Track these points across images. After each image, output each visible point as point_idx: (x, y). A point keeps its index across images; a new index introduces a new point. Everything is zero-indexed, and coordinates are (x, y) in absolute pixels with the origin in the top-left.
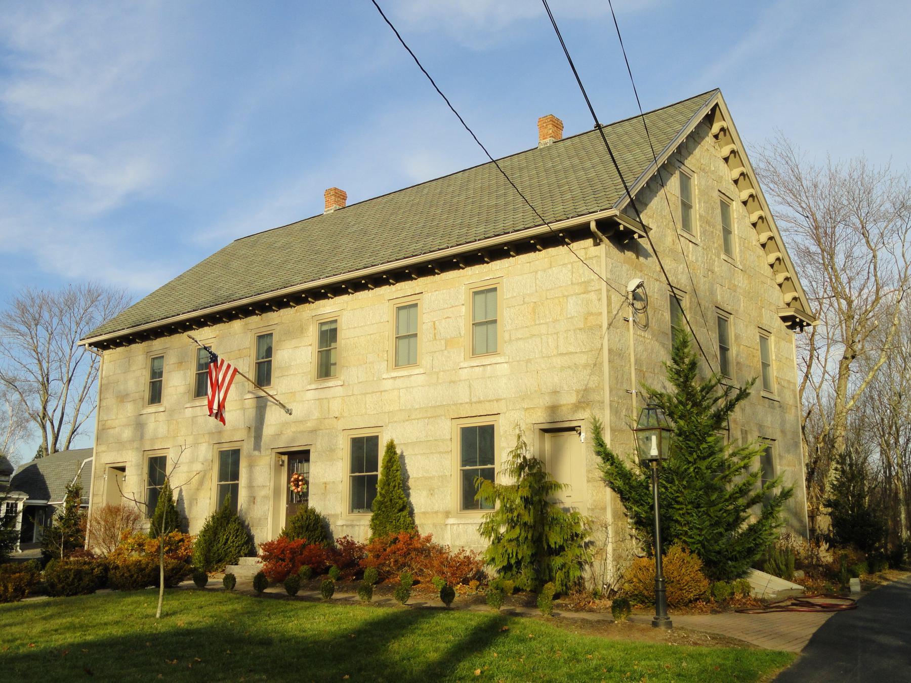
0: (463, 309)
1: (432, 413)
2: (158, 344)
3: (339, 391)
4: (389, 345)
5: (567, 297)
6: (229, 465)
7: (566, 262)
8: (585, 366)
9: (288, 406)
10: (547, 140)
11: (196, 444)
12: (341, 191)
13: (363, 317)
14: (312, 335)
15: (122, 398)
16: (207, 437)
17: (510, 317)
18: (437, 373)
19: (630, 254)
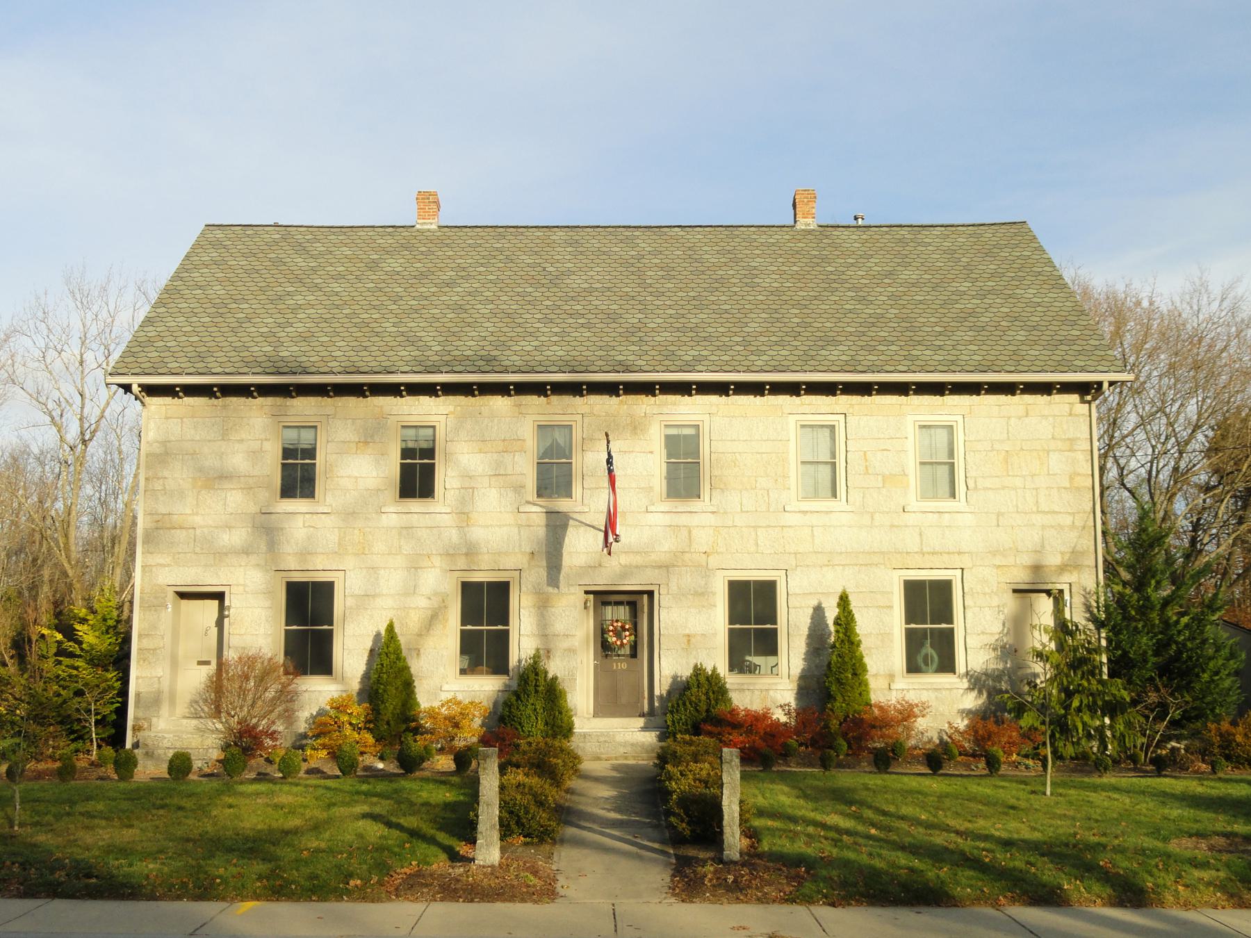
2: (304, 407)
3: (711, 520)
5: (1048, 452)
7: (1046, 413)
11: (414, 567)
14: (655, 439)
15: (217, 479)
16: (437, 561)
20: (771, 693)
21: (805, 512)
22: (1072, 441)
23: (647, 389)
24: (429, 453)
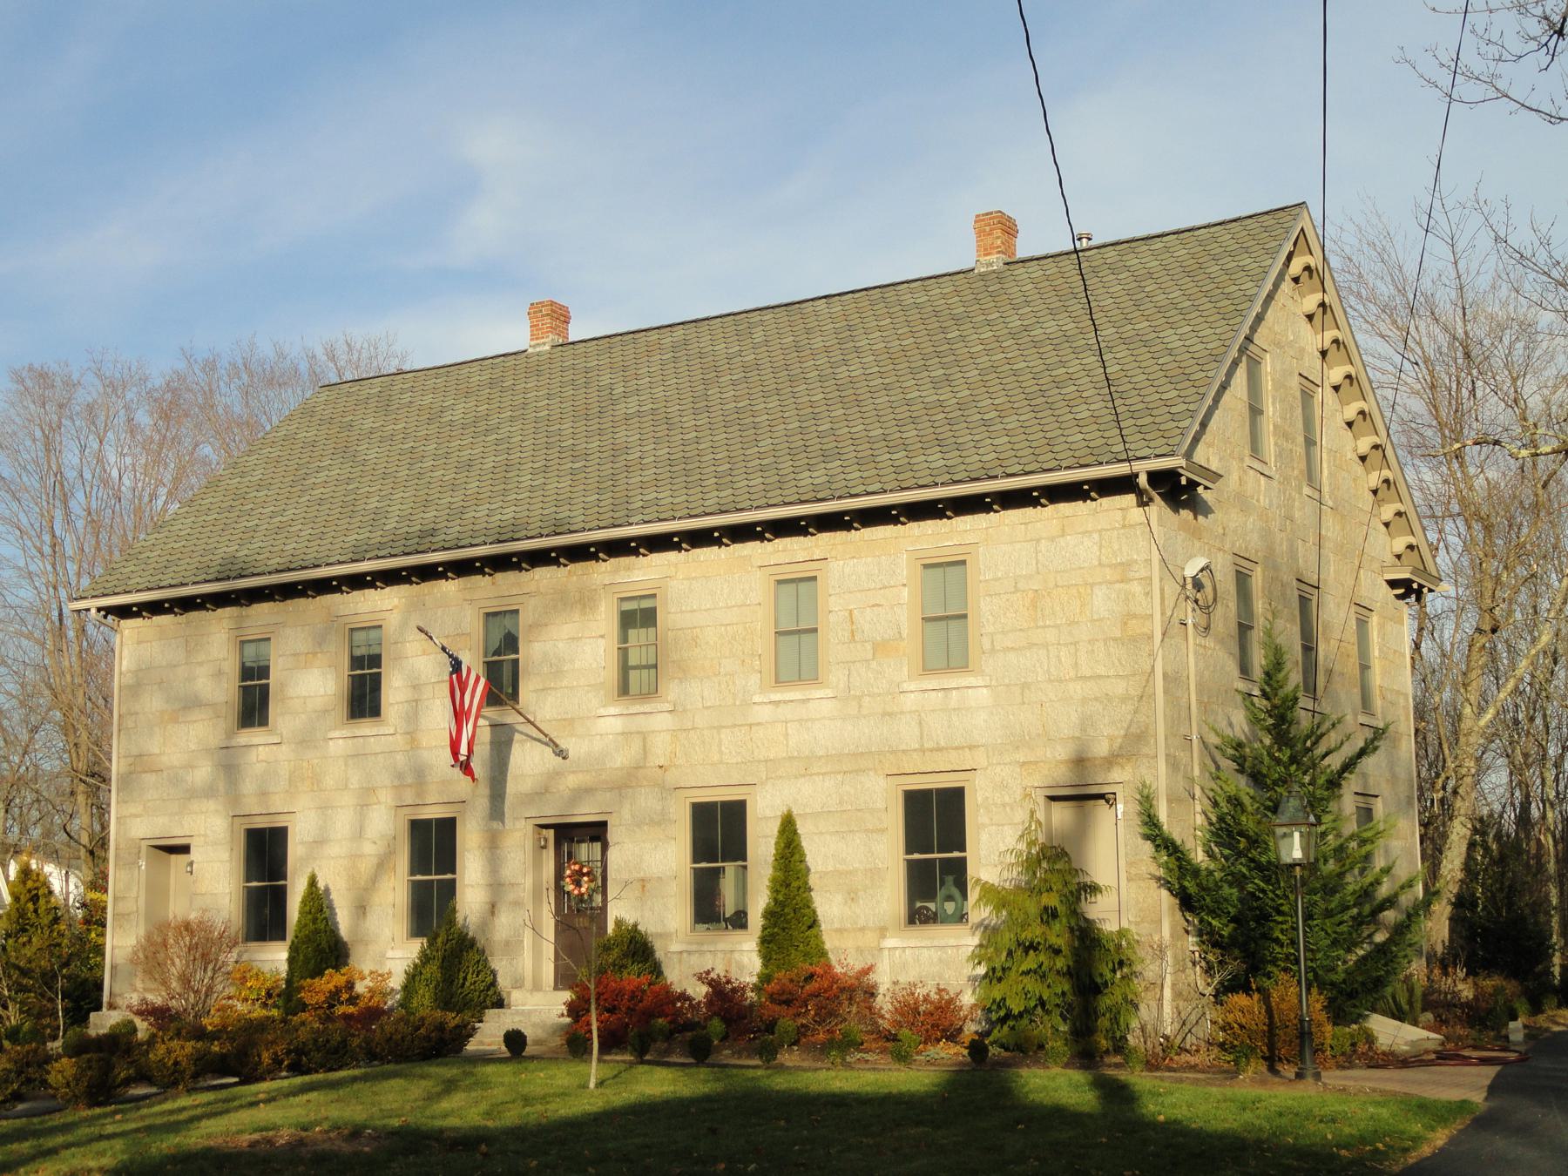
0: (905, 592)
1: (852, 762)
4: (763, 642)
5: (1092, 585)
6: (433, 844)
8: (1124, 699)
9: (563, 744)
10: (993, 258)
11: (363, 807)
12: (562, 307)
13: (714, 592)
14: (605, 619)
17: (990, 613)
18: (859, 699)
19: (1186, 514)
20: (736, 955)
21: (776, 703)
22: (1127, 565)
23: (579, 553)
24: (375, 660)
